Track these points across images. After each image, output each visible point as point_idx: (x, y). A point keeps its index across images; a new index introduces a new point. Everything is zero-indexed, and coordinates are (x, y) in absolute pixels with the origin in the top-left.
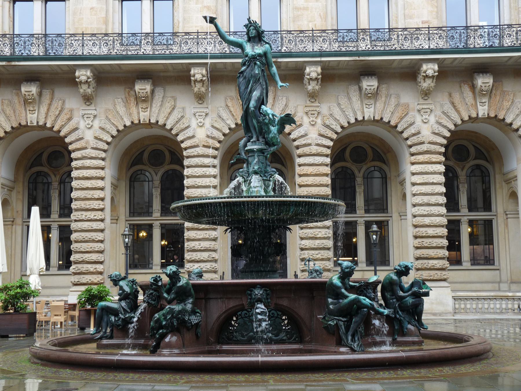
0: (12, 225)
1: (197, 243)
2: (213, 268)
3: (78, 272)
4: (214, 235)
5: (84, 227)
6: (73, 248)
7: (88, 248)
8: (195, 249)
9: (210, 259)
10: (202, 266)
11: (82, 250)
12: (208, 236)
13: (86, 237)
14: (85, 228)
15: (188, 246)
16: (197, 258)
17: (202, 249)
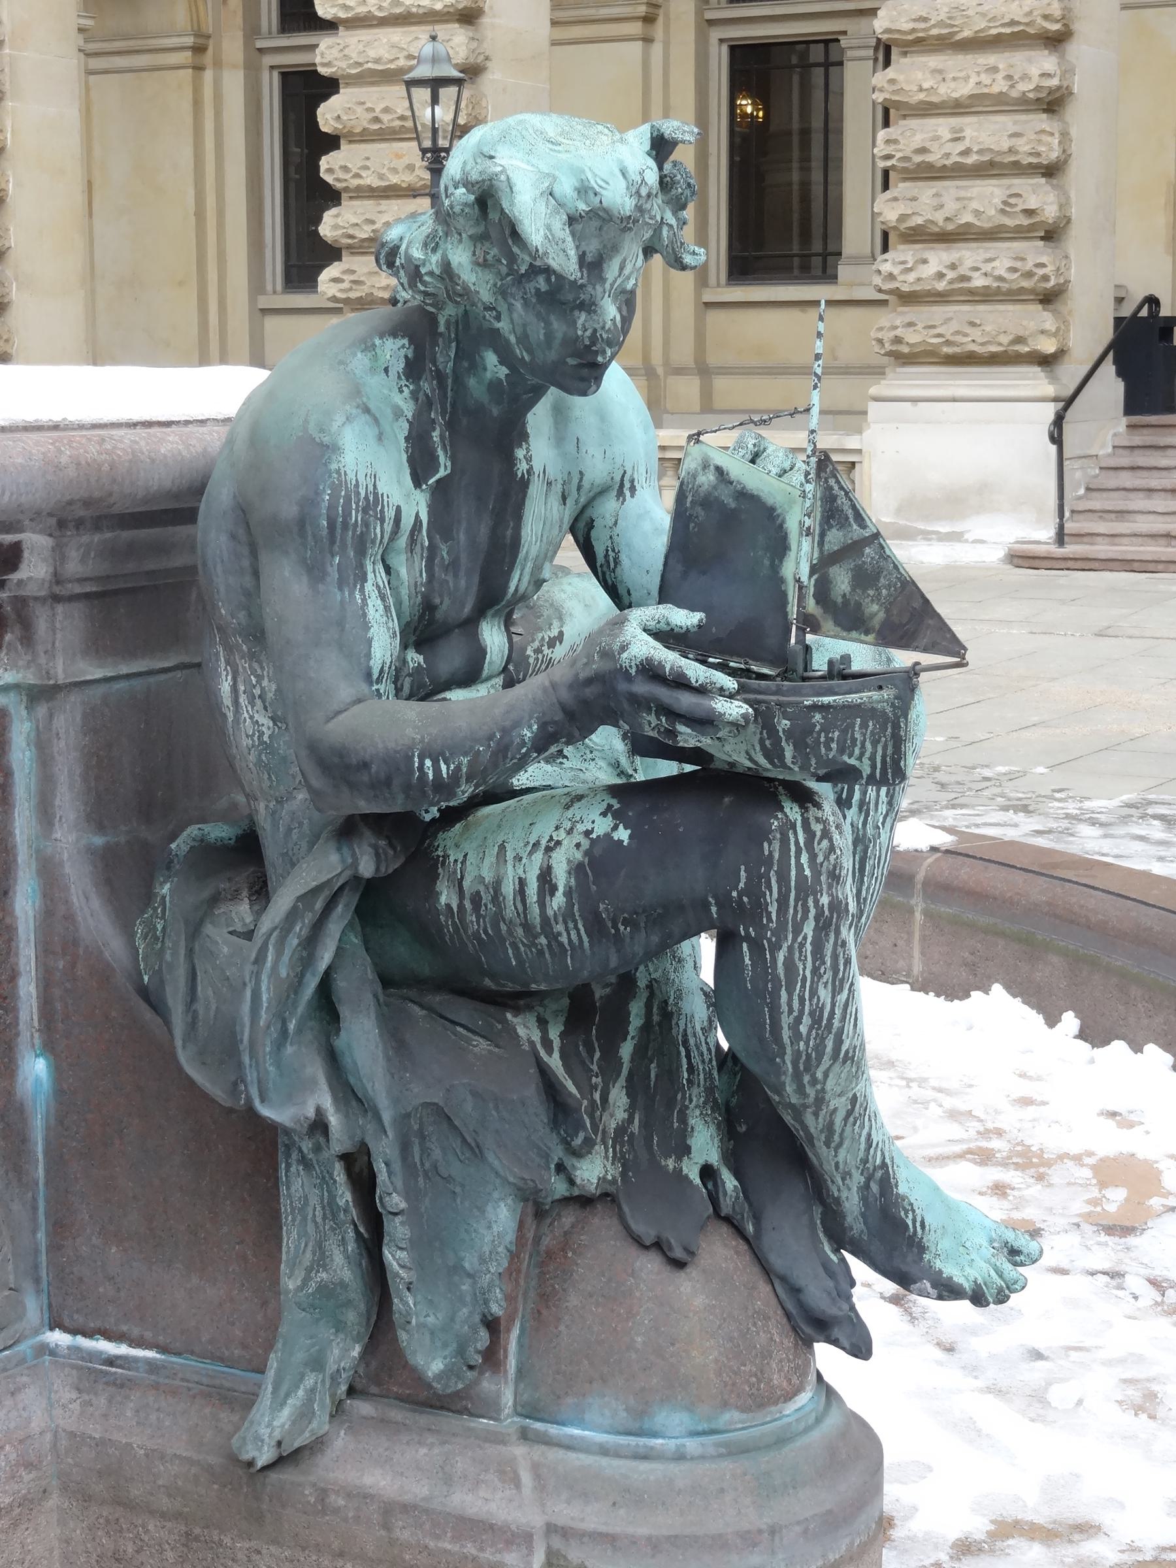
0: (199, 68)
1: (942, 126)
2: (1029, 275)
3: (353, 295)
4: (1035, 72)
5: (372, 54)
6: (330, 171)
7: (394, 171)
8: (930, 166)
9: (1010, 222)
10: (969, 263)
11: (369, 180)
12: (1000, 86)
13: (386, 110)
14: (377, 61)
15: (889, 150)
16: (939, 217)
17: (970, 160)
